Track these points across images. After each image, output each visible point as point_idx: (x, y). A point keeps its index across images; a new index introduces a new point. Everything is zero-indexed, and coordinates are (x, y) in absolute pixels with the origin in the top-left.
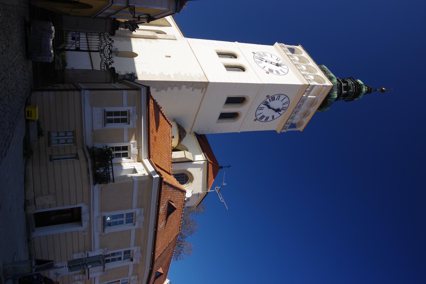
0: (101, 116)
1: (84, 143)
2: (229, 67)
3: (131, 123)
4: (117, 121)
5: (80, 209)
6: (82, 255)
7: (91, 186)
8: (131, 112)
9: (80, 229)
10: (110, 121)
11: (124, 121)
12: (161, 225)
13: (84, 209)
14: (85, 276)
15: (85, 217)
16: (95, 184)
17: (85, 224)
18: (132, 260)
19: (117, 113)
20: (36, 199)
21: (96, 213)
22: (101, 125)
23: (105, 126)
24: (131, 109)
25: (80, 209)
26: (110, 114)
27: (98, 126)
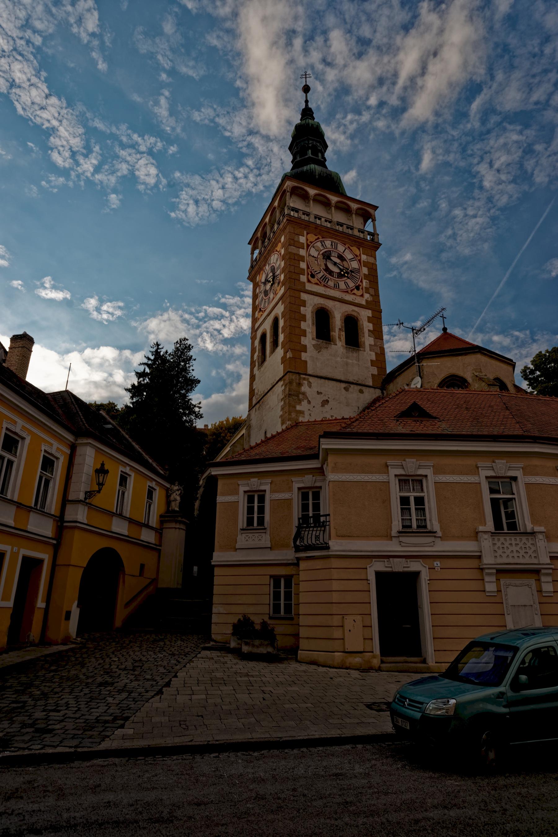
0: (250, 535)
1: (290, 562)
2: (275, 344)
3: (262, 488)
4: (261, 510)
5: (379, 574)
6: (489, 574)
7: (331, 553)
8: (247, 489)
9: (424, 576)
10: (261, 521)
11: (262, 499)
12: (442, 427)
13: (380, 566)
14: (543, 571)
15: (399, 566)
16: (328, 548)
17: (414, 566)
18: (515, 479)
19: (250, 510)
20: (349, 650)
21: (393, 547)
22: (263, 535)
23: (265, 529)
24: (242, 489)
25: (379, 574)
26: (250, 521)
27: (265, 540)
